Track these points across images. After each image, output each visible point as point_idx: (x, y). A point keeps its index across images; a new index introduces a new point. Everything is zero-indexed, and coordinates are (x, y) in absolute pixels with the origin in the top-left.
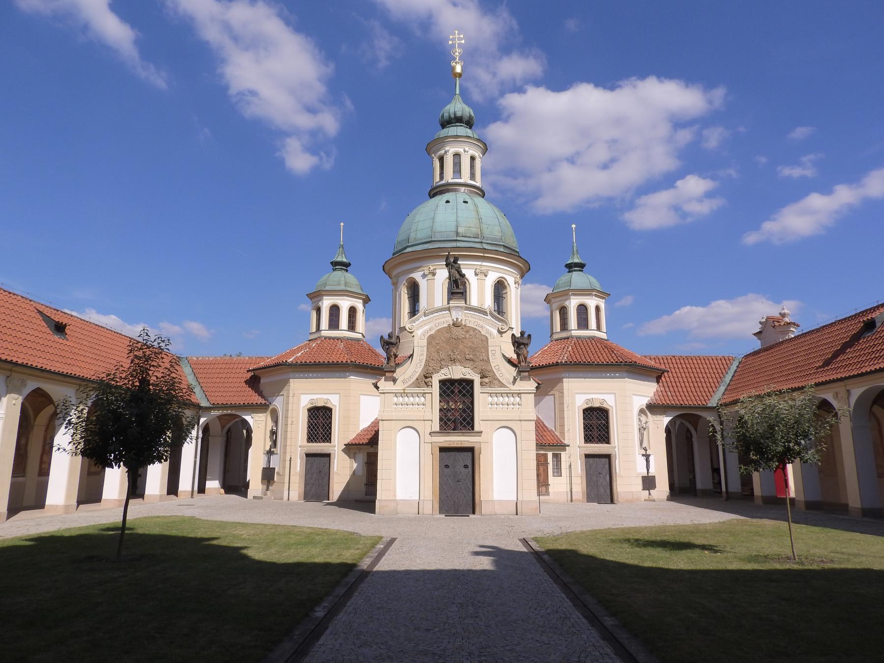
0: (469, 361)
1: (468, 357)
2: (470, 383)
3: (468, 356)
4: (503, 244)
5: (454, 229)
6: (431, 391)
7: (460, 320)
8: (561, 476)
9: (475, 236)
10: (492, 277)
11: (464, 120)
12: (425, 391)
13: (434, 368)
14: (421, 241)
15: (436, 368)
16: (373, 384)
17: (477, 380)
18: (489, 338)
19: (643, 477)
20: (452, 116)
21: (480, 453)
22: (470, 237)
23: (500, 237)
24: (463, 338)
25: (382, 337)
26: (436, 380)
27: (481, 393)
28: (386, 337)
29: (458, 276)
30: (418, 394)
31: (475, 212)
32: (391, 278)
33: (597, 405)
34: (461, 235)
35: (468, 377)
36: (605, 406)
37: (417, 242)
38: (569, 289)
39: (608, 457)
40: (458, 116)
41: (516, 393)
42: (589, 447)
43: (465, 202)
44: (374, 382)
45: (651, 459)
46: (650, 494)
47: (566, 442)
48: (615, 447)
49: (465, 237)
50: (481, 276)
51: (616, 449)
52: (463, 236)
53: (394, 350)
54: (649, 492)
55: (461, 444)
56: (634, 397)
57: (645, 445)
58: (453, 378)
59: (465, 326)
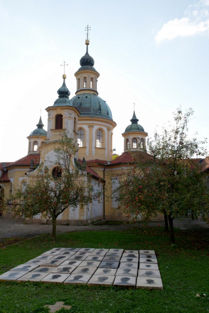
10: (96, 128)
50: (91, 128)
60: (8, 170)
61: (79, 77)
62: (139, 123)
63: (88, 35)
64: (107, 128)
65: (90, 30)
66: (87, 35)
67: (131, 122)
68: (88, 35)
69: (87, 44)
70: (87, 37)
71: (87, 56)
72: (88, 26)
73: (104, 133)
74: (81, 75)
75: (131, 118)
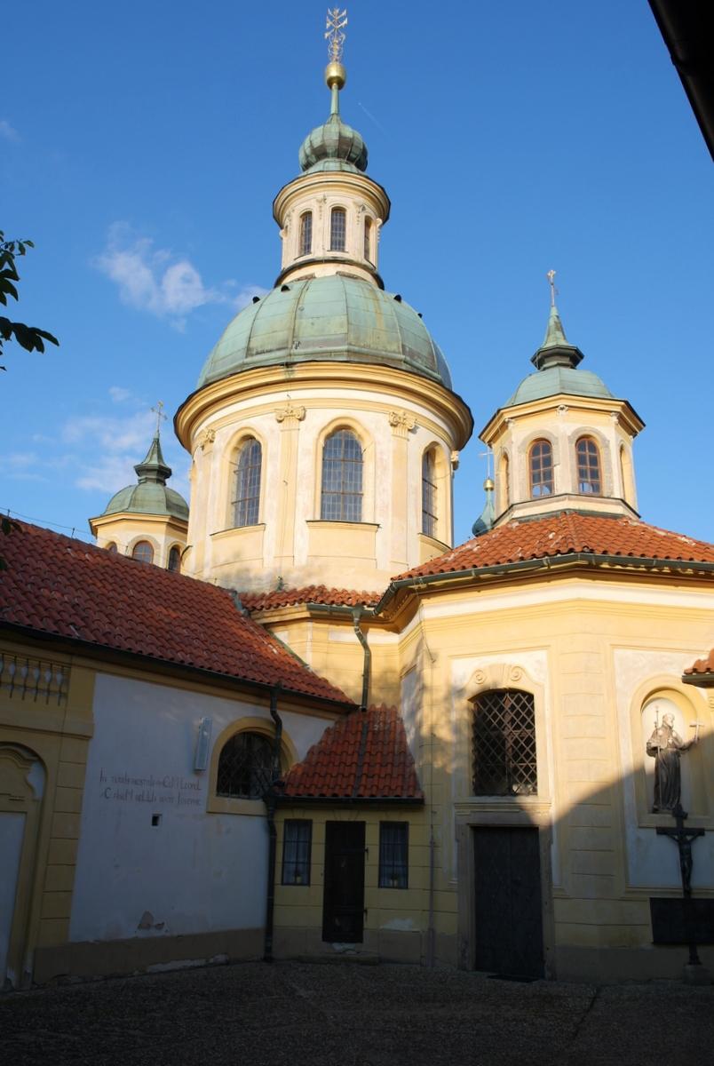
5: (244, 344)
9: (281, 346)
10: (320, 421)
11: (330, 151)
34: (254, 352)
40: (315, 147)
42: (483, 805)
46: (694, 959)
49: (263, 352)
52: (258, 353)
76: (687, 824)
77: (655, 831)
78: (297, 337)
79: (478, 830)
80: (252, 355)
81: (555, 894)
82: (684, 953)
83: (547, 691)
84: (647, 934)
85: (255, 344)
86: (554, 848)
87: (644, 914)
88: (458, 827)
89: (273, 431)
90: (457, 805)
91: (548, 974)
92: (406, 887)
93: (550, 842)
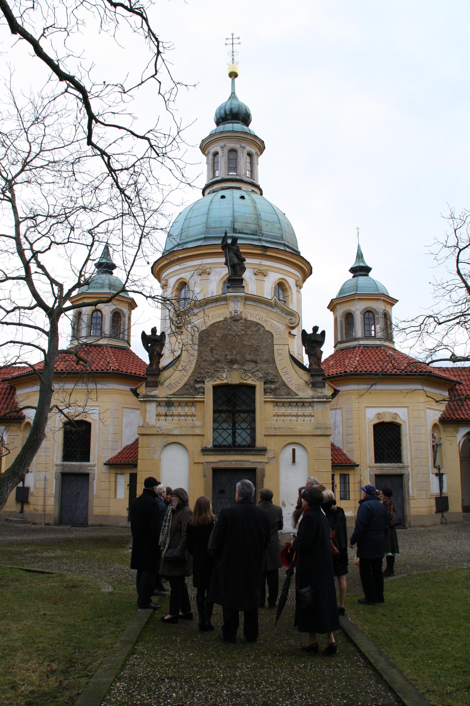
0: (250, 363)
1: (248, 357)
2: (253, 388)
3: (249, 356)
4: (283, 242)
6: (203, 400)
7: (239, 312)
8: (349, 499)
9: (253, 233)
12: (196, 399)
13: (206, 370)
14: (193, 239)
15: (209, 371)
16: (132, 390)
17: (260, 387)
18: (274, 334)
19: (436, 498)
20: (228, 112)
21: (263, 476)
22: (247, 234)
23: (280, 235)
24: (243, 335)
25: (143, 333)
26: (209, 385)
27: (265, 402)
28: (149, 333)
29: (236, 261)
30: (187, 404)
31: (253, 208)
32: (159, 281)
33: (387, 419)
34: (238, 232)
35: (250, 382)
36: (398, 421)
37: (189, 240)
38: (355, 294)
39: (401, 476)
40: (234, 112)
41: (307, 402)
42: (382, 467)
43: (243, 197)
44: (133, 388)
45: (445, 477)
46: (443, 516)
47: (357, 461)
48: (408, 467)
49: (242, 233)
50: (260, 277)
51: (410, 469)
52: (239, 233)
53: (158, 349)
54: (442, 514)
55: (240, 464)
56: (428, 411)
57: (438, 463)
58: (230, 383)
59: (246, 320)
60: (16, 388)
61: (212, 149)
62: (370, 274)
63: (233, 55)
64: (296, 281)
65: (239, 43)
66: (231, 55)
67: (352, 273)
68: (233, 55)
69: (233, 75)
70: (233, 59)
71: (234, 102)
72: (233, 35)
73: (290, 293)
74: (222, 144)
75: (352, 263)
76: (441, 472)
77: (434, 475)
78: (260, 230)
79: (377, 476)
80: (236, 233)
81: (410, 498)
82: (441, 514)
83: (407, 424)
84: (434, 509)
85: (237, 226)
86: (410, 482)
87: (433, 502)
88: (370, 475)
89: (251, 278)
90: (370, 467)
91: (408, 525)
92: (349, 499)
93: (409, 480)
